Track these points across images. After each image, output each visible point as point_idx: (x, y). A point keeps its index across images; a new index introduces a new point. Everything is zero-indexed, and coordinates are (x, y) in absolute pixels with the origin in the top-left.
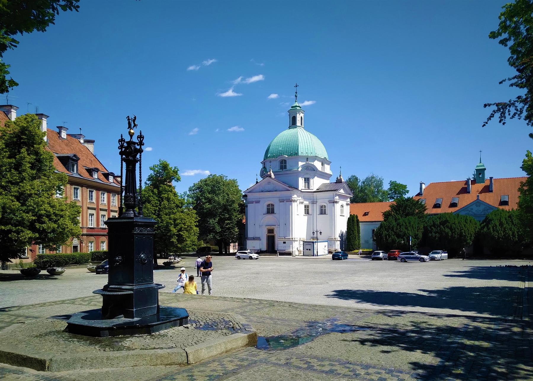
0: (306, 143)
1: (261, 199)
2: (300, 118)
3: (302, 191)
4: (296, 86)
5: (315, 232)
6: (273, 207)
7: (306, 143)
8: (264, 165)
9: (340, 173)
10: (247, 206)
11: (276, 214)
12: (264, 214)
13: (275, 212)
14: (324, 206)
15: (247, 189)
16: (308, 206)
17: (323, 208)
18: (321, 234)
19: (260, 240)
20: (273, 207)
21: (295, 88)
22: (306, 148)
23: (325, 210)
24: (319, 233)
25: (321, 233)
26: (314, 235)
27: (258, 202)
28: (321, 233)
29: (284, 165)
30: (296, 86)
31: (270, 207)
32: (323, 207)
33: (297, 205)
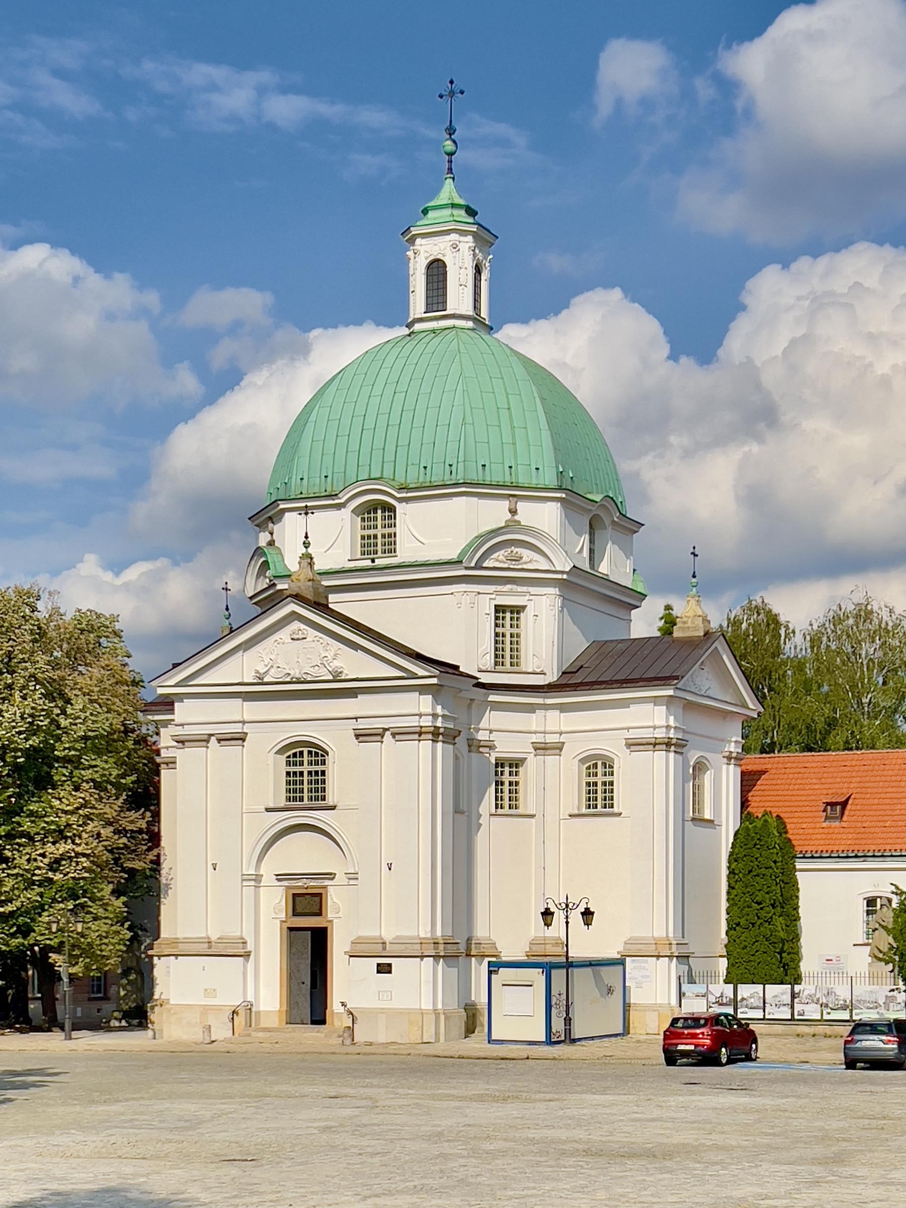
2: (471, 272)
3: (485, 679)
5: (553, 909)
6: (319, 768)
10: (171, 763)
11: (333, 808)
12: (268, 810)
16: (516, 764)
17: (600, 779)
18: (588, 923)
20: (319, 768)
24: (576, 917)
25: (587, 914)
26: (548, 924)
28: (587, 914)
29: (379, 532)
31: (306, 768)
32: (600, 770)
33: (456, 758)
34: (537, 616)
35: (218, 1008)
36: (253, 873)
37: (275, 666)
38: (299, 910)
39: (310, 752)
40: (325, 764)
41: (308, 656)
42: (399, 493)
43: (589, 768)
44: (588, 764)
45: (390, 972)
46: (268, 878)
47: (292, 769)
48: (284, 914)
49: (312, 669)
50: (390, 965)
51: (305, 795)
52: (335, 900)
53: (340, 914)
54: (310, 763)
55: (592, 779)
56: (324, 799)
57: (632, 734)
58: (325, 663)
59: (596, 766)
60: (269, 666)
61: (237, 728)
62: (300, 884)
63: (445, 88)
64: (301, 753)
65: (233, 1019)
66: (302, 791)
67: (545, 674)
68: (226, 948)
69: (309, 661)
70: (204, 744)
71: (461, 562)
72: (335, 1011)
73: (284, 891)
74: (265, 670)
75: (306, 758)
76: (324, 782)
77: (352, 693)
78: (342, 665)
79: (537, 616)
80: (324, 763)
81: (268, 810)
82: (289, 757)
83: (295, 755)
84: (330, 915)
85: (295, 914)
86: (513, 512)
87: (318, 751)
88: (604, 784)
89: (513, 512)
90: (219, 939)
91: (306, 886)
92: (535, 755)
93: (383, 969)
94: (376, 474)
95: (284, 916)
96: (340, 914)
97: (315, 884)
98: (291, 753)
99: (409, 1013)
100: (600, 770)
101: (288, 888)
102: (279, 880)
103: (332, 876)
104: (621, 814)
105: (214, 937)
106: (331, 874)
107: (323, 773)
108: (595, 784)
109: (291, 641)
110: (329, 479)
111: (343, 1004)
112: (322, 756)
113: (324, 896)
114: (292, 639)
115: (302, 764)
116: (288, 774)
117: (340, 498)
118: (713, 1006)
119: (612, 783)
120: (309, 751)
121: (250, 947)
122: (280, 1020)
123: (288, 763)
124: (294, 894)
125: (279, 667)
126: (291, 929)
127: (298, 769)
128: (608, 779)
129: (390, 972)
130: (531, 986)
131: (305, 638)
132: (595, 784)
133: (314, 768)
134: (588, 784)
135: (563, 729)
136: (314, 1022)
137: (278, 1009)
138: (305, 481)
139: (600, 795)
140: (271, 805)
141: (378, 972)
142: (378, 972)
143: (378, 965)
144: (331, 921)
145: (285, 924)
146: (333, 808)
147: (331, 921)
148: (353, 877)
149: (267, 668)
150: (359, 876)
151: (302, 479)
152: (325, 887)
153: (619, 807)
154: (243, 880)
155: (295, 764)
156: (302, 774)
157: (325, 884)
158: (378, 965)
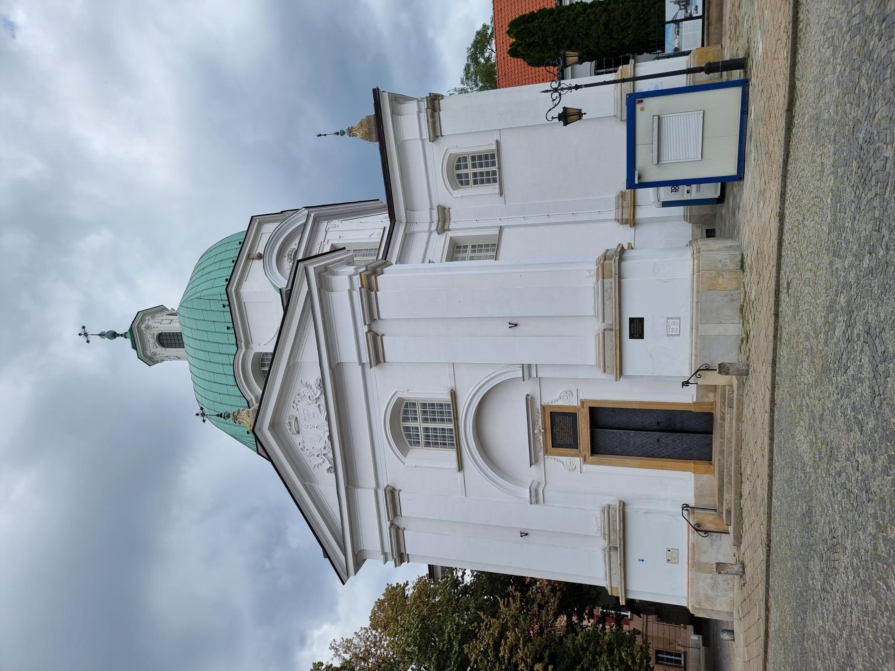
0: (206, 271)
1: (384, 483)
4: (86, 335)
6: (419, 409)
7: (206, 271)
9: (343, 133)
11: (453, 394)
12: (461, 467)
13: (446, 398)
15: (326, 555)
17: (470, 171)
20: (419, 409)
21: (91, 338)
22: (217, 266)
27: (392, 494)
30: (86, 335)
32: (463, 171)
34: (340, 237)
35: (693, 549)
37: (324, 452)
38: (570, 440)
39: (406, 419)
40: (415, 403)
41: (312, 416)
42: (242, 348)
43: (461, 183)
44: (458, 183)
45: (641, 320)
47: (422, 440)
48: (575, 458)
50: (632, 320)
53: (574, 390)
55: (471, 179)
57: (426, 135)
58: (315, 398)
59: (459, 176)
60: (324, 458)
61: (381, 493)
62: (541, 437)
63: (83, 339)
64: (407, 429)
65: (706, 532)
67: (385, 228)
68: (615, 532)
69: (315, 414)
70: (401, 532)
71: (280, 289)
72: (695, 401)
73: (550, 457)
74: (327, 461)
75: (411, 424)
77: (337, 369)
78: (316, 378)
79: (340, 237)
81: (461, 467)
82: (410, 443)
83: (409, 436)
85: (573, 444)
86: (260, 257)
88: (474, 166)
89: (260, 257)
90: (604, 538)
91: (542, 431)
92: (449, 230)
93: (637, 328)
94: (230, 370)
96: (574, 390)
97: (540, 420)
99: (698, 292)
100: (463, 171)
101: (546, 452)
102: (536, 461)
103: (529, 398)
106: (527, 399)
107: (424, 405)
108: (475, 175)
109: (300, 432)
111: (686, 383)
112: (406, 406)
114: (298, 433)
116: (428, 444)
117: (252, 400)
118: (689, 11)
119: (473, 158)
120: (403, 421)
122: (707, 472)
124: (552, 447)
126: (594, 451)
127: (422, 434)
128: (469, 162)
129: (641, 320)
130: (659, 118)
131: (296, 418)
132: (475, 175)
133: (419, 416)
134: (475, 182)
135: (428, 206)
136: (709, 432)
137: (693, 475)
139: (484, 169)
140: (455, 465)
141: (641, 336)
142: (641, 336)
143: (632, 336)
144: (583, 402)
145: (587, 456)
146: (453, 394)
147: (583, 402)
148: (527, 369)
149: (326, 459)
150: (526, 362)
153: (491, 144)
154: (537, 502)
156: (426, 429)
157: (539, 407)
158: (630, 338)
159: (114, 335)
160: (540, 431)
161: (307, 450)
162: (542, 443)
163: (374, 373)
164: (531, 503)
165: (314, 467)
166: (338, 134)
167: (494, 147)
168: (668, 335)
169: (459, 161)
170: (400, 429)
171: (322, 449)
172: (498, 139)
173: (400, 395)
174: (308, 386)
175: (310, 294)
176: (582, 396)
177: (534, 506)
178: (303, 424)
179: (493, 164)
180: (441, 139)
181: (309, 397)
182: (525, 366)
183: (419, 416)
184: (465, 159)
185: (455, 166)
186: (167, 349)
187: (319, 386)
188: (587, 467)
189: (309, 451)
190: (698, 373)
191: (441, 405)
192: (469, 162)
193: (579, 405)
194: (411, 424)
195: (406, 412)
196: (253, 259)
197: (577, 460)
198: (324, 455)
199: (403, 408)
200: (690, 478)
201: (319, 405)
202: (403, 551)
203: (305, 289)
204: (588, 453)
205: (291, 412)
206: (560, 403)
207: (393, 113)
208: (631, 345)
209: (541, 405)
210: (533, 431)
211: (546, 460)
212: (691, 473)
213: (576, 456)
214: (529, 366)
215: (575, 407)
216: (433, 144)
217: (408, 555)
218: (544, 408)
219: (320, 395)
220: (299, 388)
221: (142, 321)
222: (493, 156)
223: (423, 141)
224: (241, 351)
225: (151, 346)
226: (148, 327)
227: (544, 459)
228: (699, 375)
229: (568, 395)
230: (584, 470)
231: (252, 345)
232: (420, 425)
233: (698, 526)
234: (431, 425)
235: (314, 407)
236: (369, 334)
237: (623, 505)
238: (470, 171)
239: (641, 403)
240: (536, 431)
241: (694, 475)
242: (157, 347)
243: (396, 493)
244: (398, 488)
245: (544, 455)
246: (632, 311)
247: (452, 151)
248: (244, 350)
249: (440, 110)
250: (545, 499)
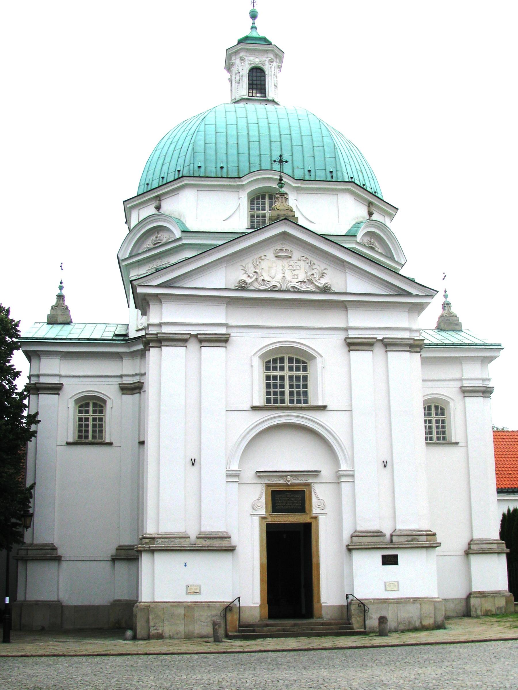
1: (234, 334)
6: (301, 373)
8: (158, 208)
14: (437, 408)
17: (434, 418)
19: (231, 550)
20: (301, 373)
23: (442, 425)
32: (433, 411)
35: (209, 605)
36: (237, 469)
39: (291, 360)
41: (294, 273)
42: (296, 183)
45: (396, 563)
46: (248, 475)
47: (272, 373)
48: (264, 510)
49: (297, 284)
50: (396, 557)
51: (287, 397)
52: (320, 497)
54: (291, 369)
56: (306, 401)
57: (466, 383)
61: (222, 330)
62: (282, 481)
64: (282, 360)
65: (225, 616)
66: (282, 394)
69: (296, 277)
72: (323, 605)
75: (286, 365)
76: (305, 386)
80: (305, 369)
81: (255, 408)
82: (269, 362)
83: (275, 361)
84: (315, 511)
86: (370, 214)
87: (297, 357)
95: (264, 512)
98: (271, 358)
100: (433, 411)
101: (268, 485)
102: (259, 476)
103: (319, 474)
104: (457, 443)
105: (193, 534)
107: (305, 378)
109: (276, 259)
110: (225, 170)
112: (304, 362)
113: (307, 493)
114: (277, 257)
115: (282, 369)
116: (268, 378)
117: (242, 181)
119: (443, 421)
121: (235, 541)
123: (268, 368)
125: (263, 280)
127: (278, 373)
128: (440, 418)
129: (396, 563)
131: (290, 257)
133: (295, 373)
137: (258, 605)
138: (202, 169)
143: (384, 557)
145: (265, 520)
146: (323, 408)
147: (316, 518)
149: (253, 280)
151: (199, 167)
152: (308, 485)
154: (227, 476)
155: (275, 369)
156: (282, 378)
157: (310, 481)
159: (254, 16)
160: (289, 481)
161: (260, 262)
162: (277, 482)
163: (339, 338)
164: (226, 471)
165: (242, 266)
166: (445, 292)
167: (454, 441)
168: (385, 583)
169: (442, 409)
170: (282, 353)
171: (262, 278)
172: (460, 444)
173: (319, 359)
174: (323, 275)
175: (409, 294)
176: (321, 518)
177: (224, 473)
178: (285, 262)
179: (438, 438)
180: (461, 395)
181: (313, 274)
182: (352, 472)
183: (295, 373)
184: (443, 414)
185: (438, 405)
186: (248, 74)
187: (326, 287)
188: (257, 520)
189: (259, 263)
190: (362, 605)
191: (306, 394)
192: (440, 418)
193: (314, 515)
194: (286, 365)
195: (298, 361)
196: (369, 207)
197: (263, 512)
198: (256, 278)
199: (301, 359)
200: (255, 603)
201: (305, 282)
202: (164, 343)
203: (414, 292)
204: (270, 520)
205: (297, 254)
206: (314, 500)
207: (484, 357)
208: (377, 557)
209: (311, 483)
210: (289, 475)
211: (260, 486)
212: (260, 604)
213: (266, 511)
214: (353, 476)
215: (311, 510)
216: (458, 389)
217: (160, 347)
218: (308, 485)
219: (316, 285)
220: (320, 266)
221: (276, 56)
222: (444, 438)
223: (461, 380)
224: (293, 182)
225: (251, 58)
226: (271, 61)
227: (262, 483)
228: (360, 606)
229: (322, 506)
230: (254, 517)
231: (295, 193)
232: (286, 373)
233: (230, 609)
234: (287, 382)
235: (302, 277)
236: (375, 340)
237: (231, 550)
238: (434, 418)
239: (318, 565)
240: (289, 478)
241: (257, 606)
242: (250, 64)
243: (223, 344)
244: (228, 345)
245: (265, 483)
246: (403, 556)
247: (452, 404)
248: (294, 185)
249: (483, 397)
250: (229, 483)
